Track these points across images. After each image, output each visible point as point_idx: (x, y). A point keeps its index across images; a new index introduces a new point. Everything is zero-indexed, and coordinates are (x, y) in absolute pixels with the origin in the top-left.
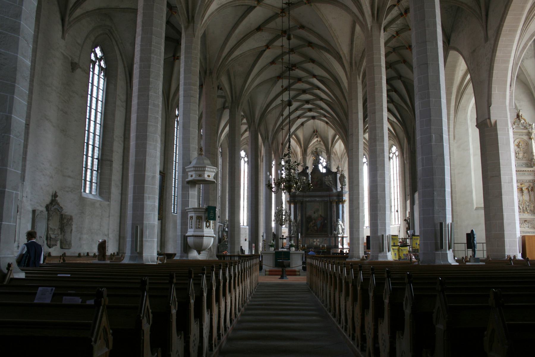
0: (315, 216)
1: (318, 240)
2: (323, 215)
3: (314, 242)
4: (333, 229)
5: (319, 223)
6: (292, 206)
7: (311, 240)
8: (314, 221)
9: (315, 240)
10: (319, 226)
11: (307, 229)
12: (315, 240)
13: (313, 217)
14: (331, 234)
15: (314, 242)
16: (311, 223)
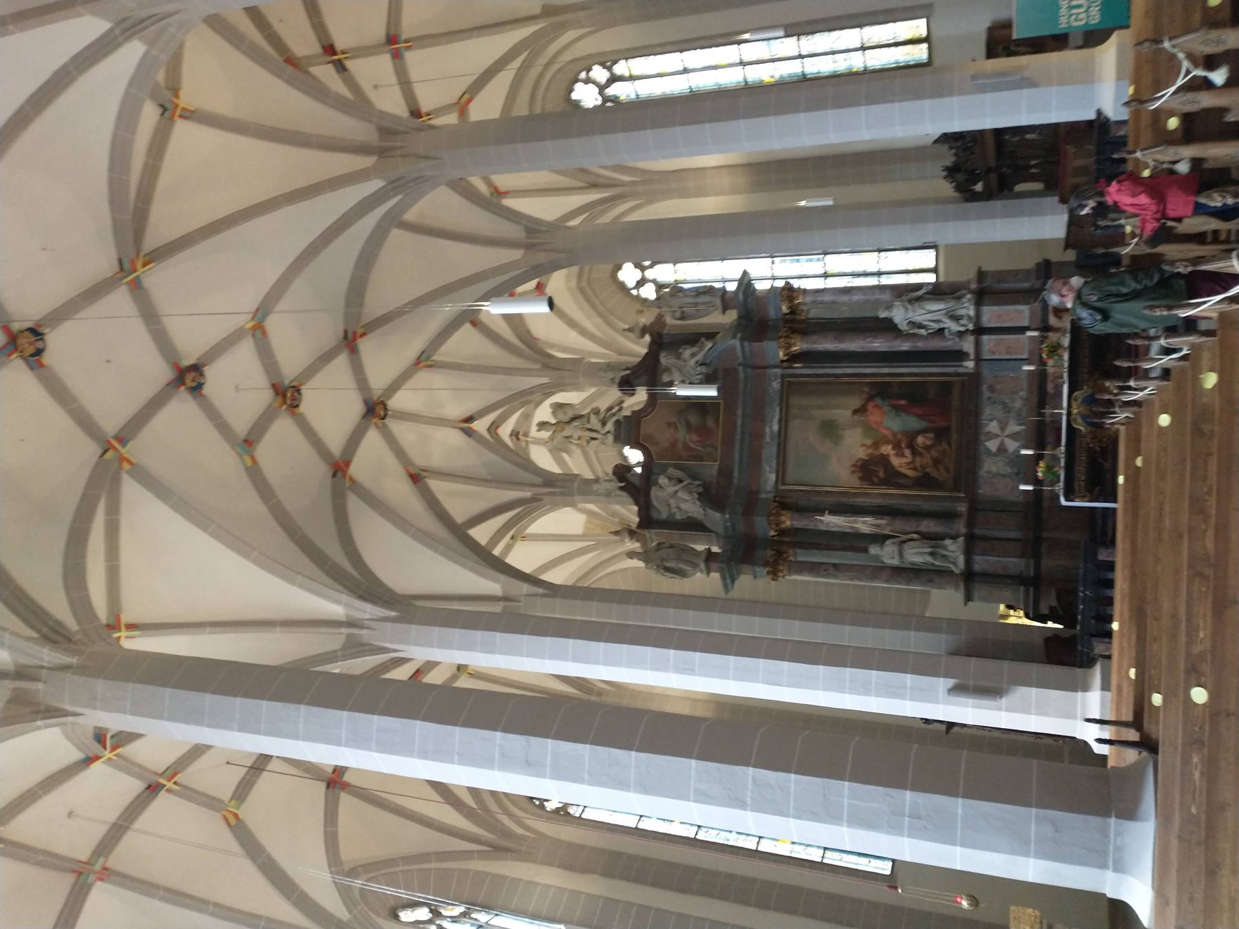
0: (855, 444)
1: (993, 427)
2: (856, 402)
3: (1002, 449)
4: (937, 344)
5: (892, 423)
6: (802, 556)
7: (989, 466)
8: (887, 449)
9: (992, 445)
10: (913, 423)
11: (925, 481)
12: (992, 445)
13: (862, 454)
14: (960, 356)
15: (1002, 449)
16: (896, 461)
